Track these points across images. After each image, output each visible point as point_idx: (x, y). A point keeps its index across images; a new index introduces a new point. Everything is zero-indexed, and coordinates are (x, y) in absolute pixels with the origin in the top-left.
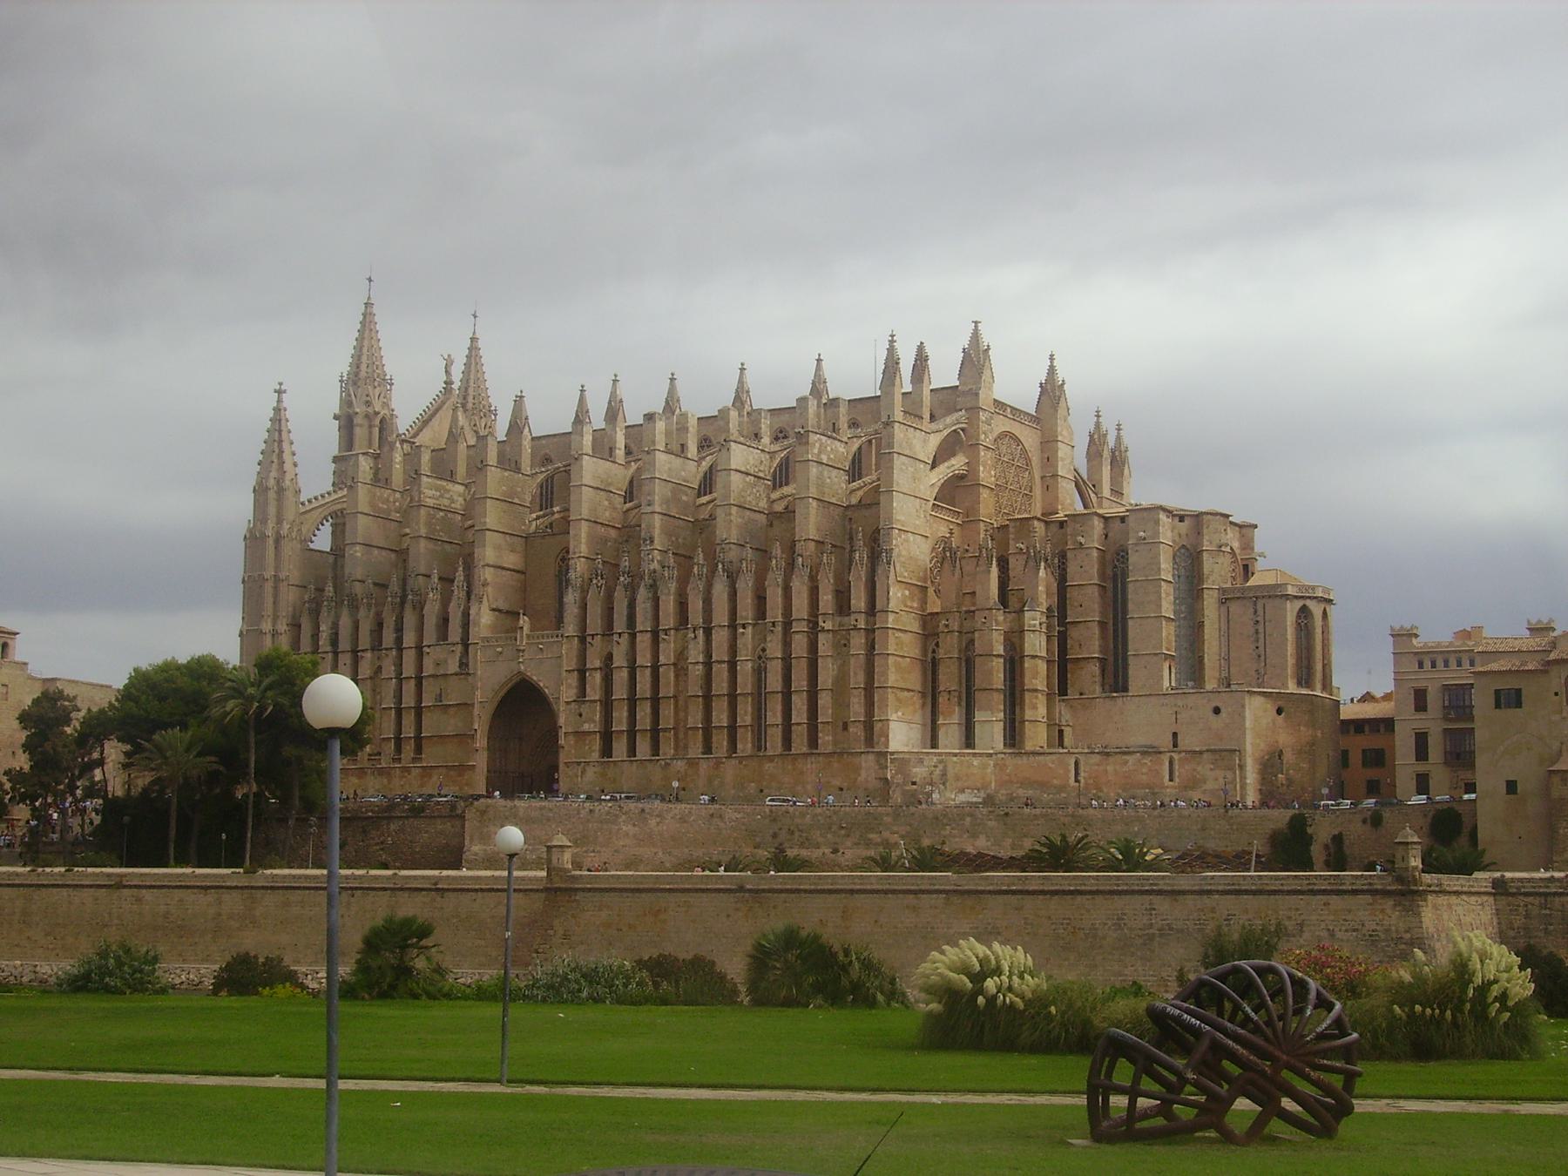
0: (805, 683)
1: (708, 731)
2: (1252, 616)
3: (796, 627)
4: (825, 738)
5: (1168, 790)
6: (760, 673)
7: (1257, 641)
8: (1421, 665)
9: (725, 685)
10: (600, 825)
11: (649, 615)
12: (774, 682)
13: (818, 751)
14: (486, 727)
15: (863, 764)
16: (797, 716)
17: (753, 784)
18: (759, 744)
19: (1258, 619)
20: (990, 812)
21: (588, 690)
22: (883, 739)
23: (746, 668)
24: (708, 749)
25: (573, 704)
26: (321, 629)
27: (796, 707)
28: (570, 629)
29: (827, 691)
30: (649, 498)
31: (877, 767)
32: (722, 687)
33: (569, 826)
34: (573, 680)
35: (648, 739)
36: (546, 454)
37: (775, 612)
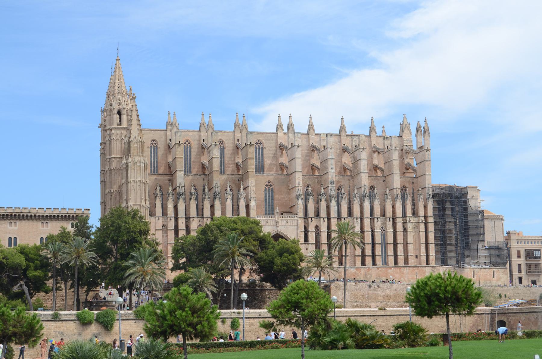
0: (402, 241)
1: (363, 256)
4: (412, 261)
5: (494, 281)
8: (518, 243)
11: (336, 212)
12: (390, 240)
13: (409, 266)
15: (427, 271)
17: (384, 277)
18: (385, 262)
24: (363, 263)
25: (303, 245)
26: (168, 206)
30: (332, 166)
33: (363, 292)
36: (221, 139)
37: (389, 214)
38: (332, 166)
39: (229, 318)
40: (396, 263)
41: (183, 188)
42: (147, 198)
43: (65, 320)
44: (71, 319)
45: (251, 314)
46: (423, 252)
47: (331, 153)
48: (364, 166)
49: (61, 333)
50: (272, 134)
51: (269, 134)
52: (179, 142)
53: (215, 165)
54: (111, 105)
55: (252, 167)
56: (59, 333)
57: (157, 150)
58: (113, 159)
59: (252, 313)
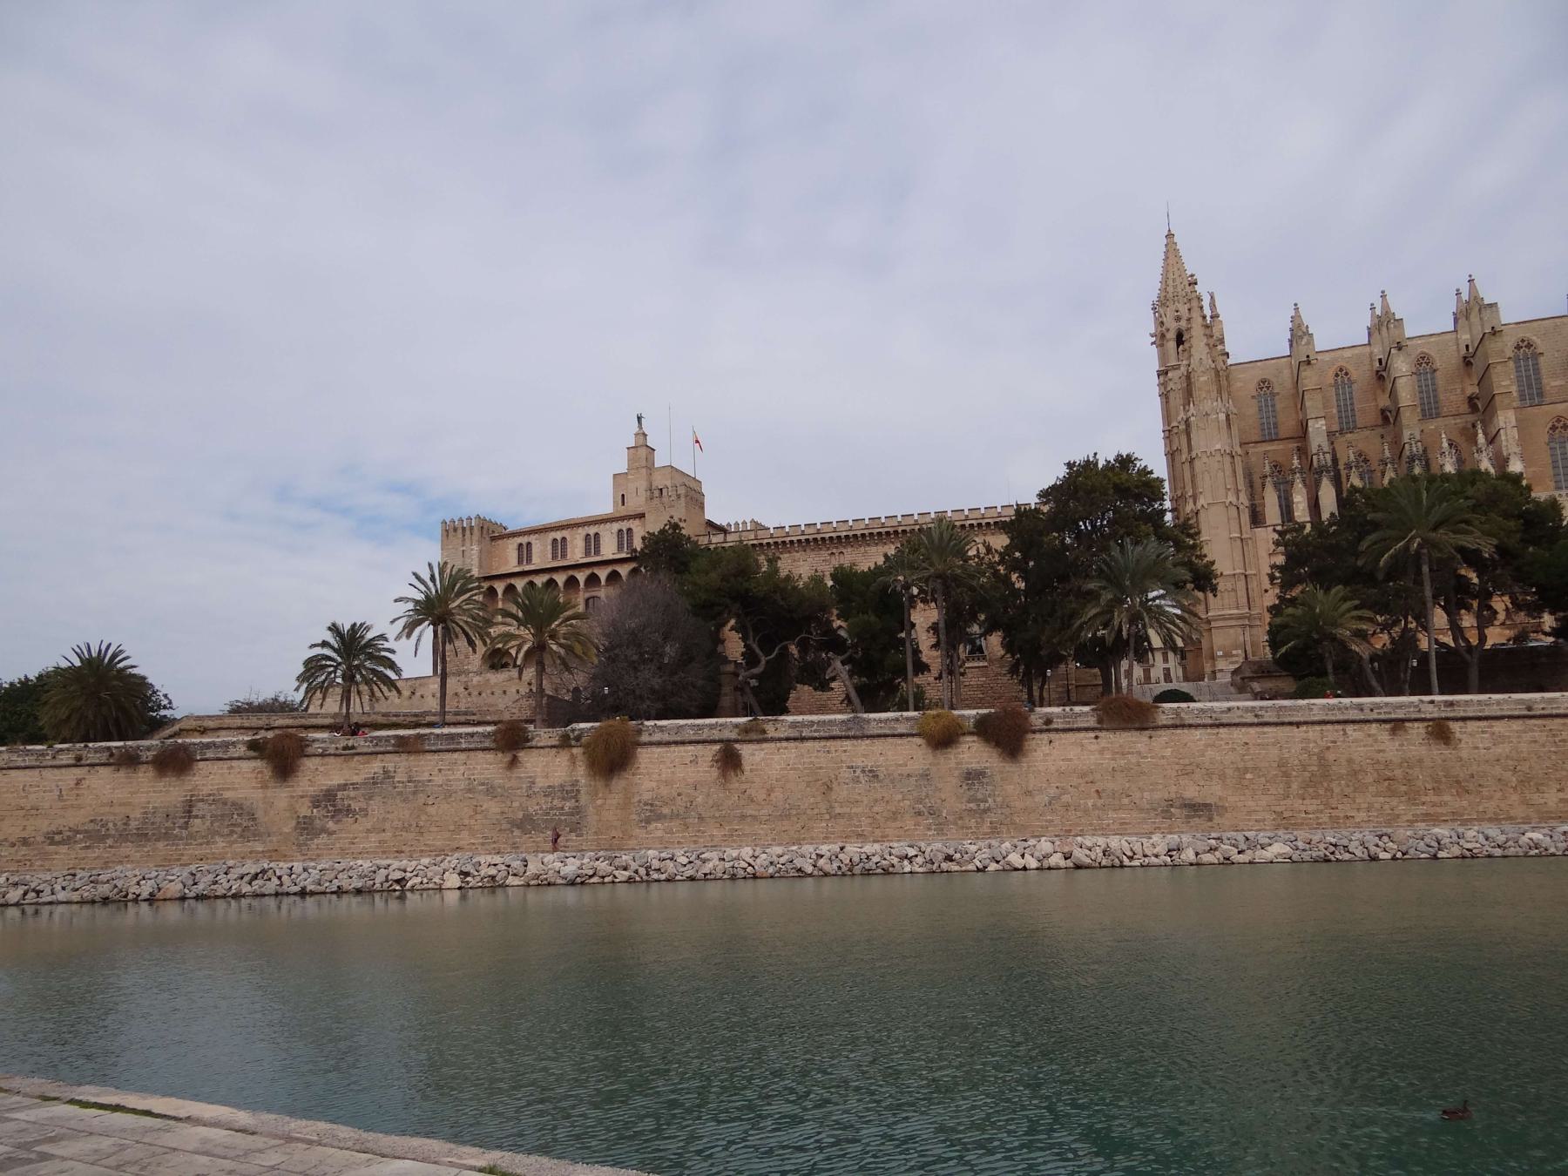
39: (1416, 720)
41: (1328, 457)
42: (1240, 488)
43: (879, 736)
44: (896, 732)
45: (1495, 707)
49: (870, 771)
50: (1557, 320)
51: (1547, 322)
52: (1308, 356)
53: (1404, 394)
54: (1162, 323)
55: (1503, 383)
56: (863, 771)
57: (1272, 400)
58: (1175, 430)
59: (1498, 703)
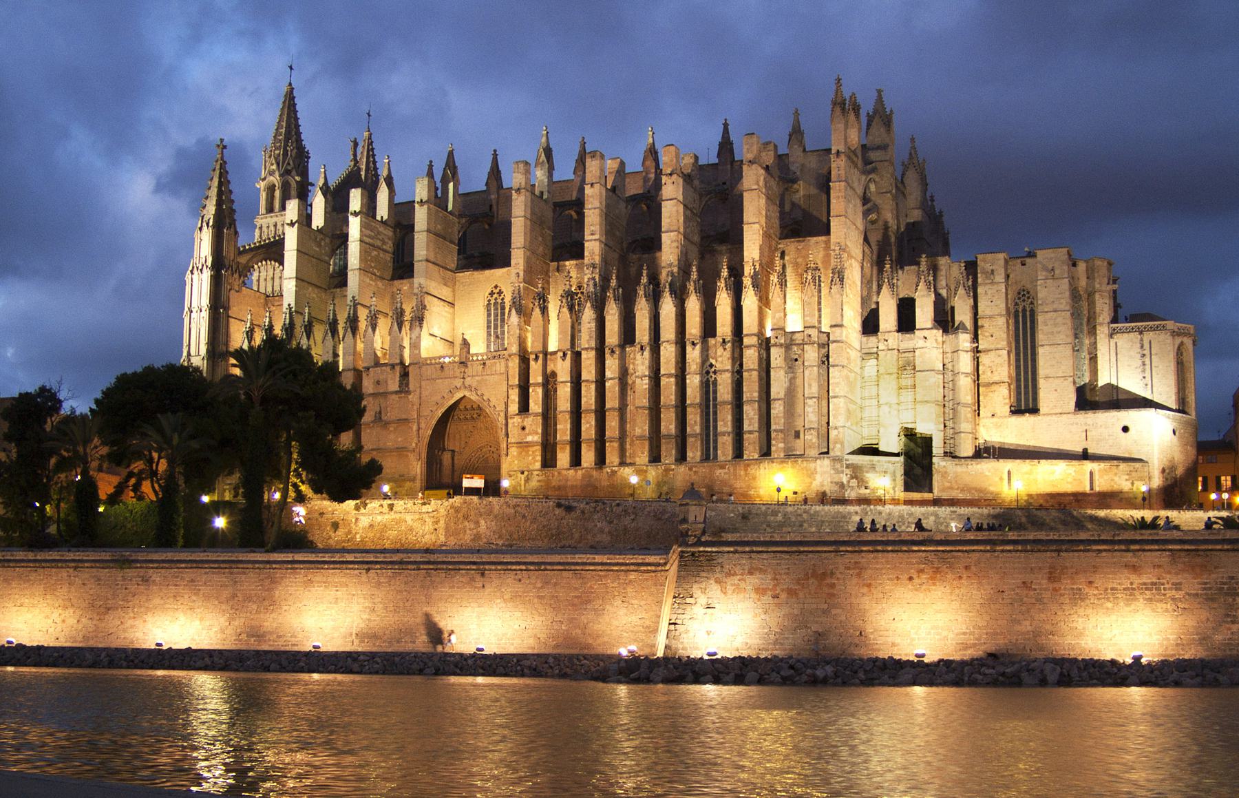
0: (756, 394)
2: (1139, 350)
3: (746, 341)
4: (777, 446)
6: (708, 387)
7: (1144, 371)
9: (673, 397)
10: (575, 522)
12: (724, 391)
14: (426, 441)
15: (819, 469)
16: (749, 425)
19: (1145, 352)
20: (951, 512)
21: (532, 404)
22: (838, 446)
23: (693, 381)
27: (747, 416)
28: (513, 348)
29: (780, 402)
30: (592, 228)
31: (832, 472)
32: (671, 400)
34: (515, 396)
35: (593, 450)
38: (592, 228)
40: (738, 453)
46: (812, 422)
47: (592, 196)
48: (670, 217)
